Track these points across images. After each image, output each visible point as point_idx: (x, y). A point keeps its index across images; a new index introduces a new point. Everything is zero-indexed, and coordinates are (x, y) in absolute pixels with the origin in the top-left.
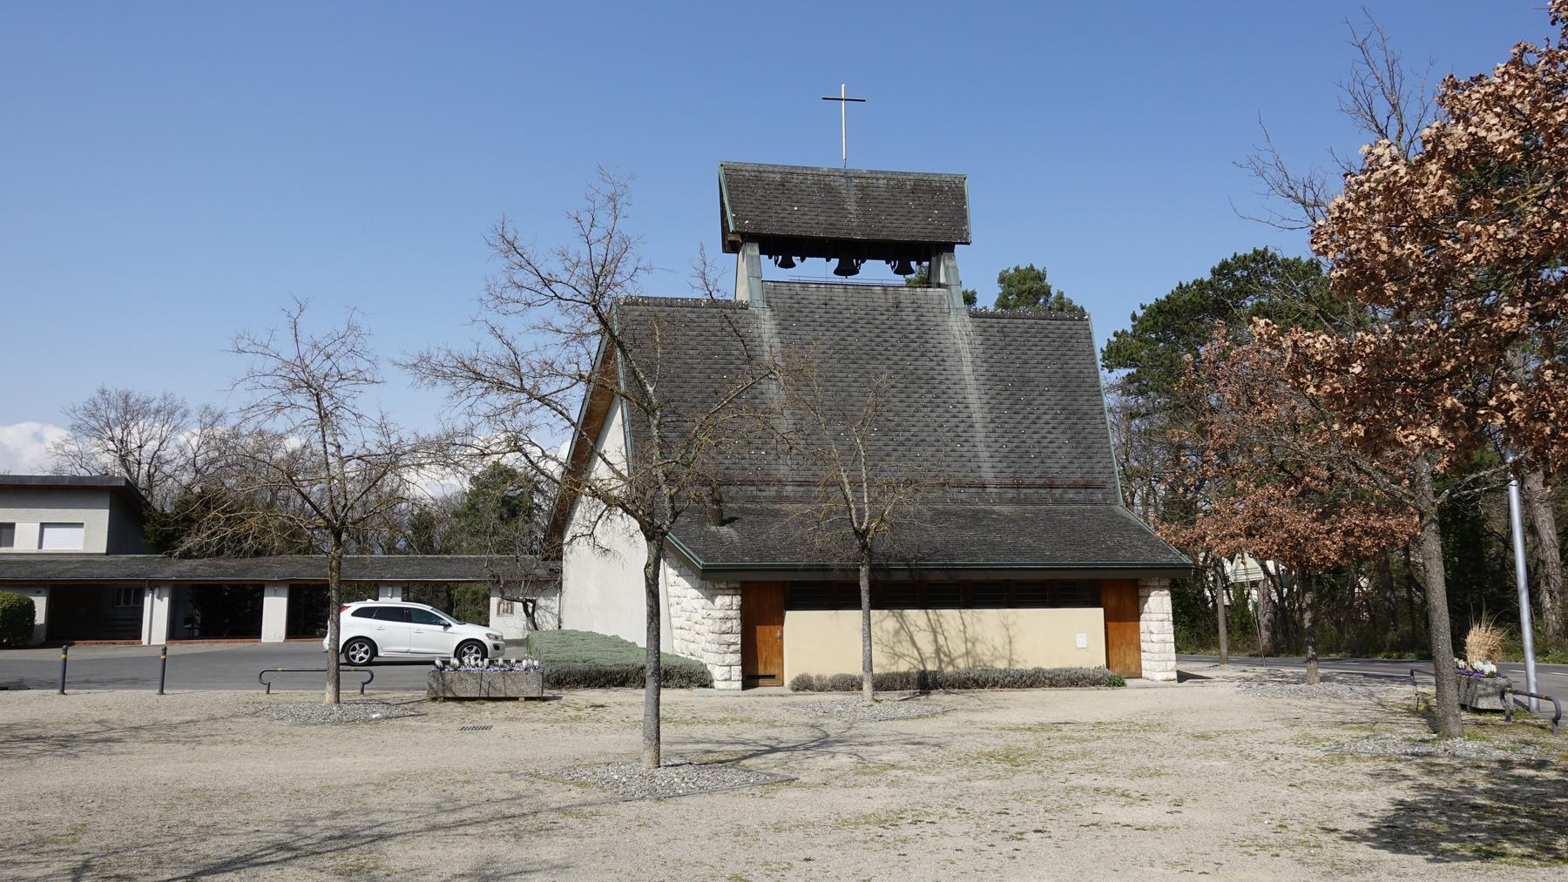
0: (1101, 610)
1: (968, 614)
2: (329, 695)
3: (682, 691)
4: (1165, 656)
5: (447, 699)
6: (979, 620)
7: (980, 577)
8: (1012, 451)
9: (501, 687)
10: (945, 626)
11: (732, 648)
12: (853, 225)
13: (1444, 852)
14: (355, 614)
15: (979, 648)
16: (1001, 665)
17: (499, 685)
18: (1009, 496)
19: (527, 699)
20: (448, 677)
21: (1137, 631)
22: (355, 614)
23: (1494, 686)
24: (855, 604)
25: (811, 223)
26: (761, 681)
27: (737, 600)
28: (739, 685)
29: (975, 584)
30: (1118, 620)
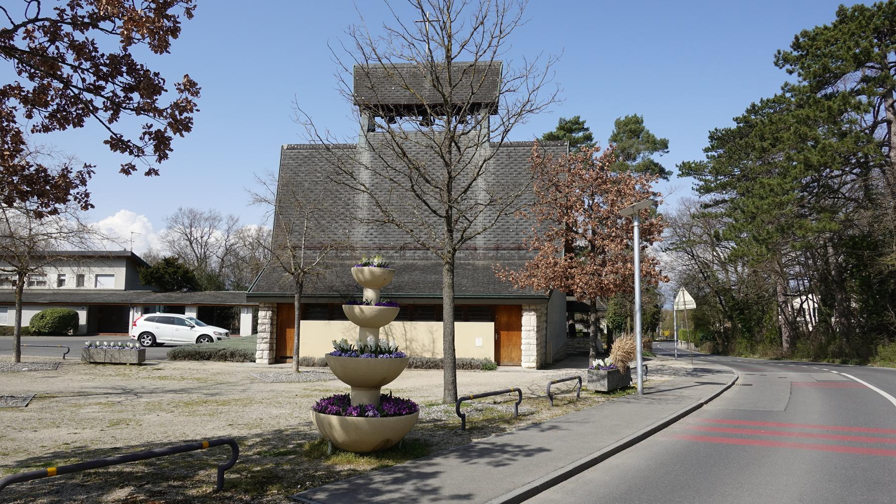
0: (492, 325)
1: (408, 324)
2: (13, 358)
3: (239, 364)
4: (530, 353)
5: (91, 363)
6: (415, 328)
7: (411, 302)
8: (499, 228)
9: (118, 358)
10: (394, 331)
11: (265, 340)
12: (426, 94)
13: (402, 472)
14: (146, 320)
15: (414, 345)
16: (428, 355)
17: (117, 356)
18: (491, 255)
19: (131, 364)
20: (91, 351)
21: (520, 338)
22: (146, 320)
23: (597, 375)
24: (439, 318)
25: (402, 98)
26: (288, 360)
27: (269, 313)
28: (266, 361)
29: (469, 306)
30: (508, 330)
